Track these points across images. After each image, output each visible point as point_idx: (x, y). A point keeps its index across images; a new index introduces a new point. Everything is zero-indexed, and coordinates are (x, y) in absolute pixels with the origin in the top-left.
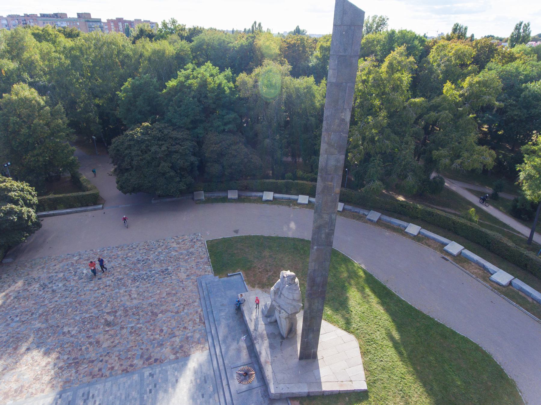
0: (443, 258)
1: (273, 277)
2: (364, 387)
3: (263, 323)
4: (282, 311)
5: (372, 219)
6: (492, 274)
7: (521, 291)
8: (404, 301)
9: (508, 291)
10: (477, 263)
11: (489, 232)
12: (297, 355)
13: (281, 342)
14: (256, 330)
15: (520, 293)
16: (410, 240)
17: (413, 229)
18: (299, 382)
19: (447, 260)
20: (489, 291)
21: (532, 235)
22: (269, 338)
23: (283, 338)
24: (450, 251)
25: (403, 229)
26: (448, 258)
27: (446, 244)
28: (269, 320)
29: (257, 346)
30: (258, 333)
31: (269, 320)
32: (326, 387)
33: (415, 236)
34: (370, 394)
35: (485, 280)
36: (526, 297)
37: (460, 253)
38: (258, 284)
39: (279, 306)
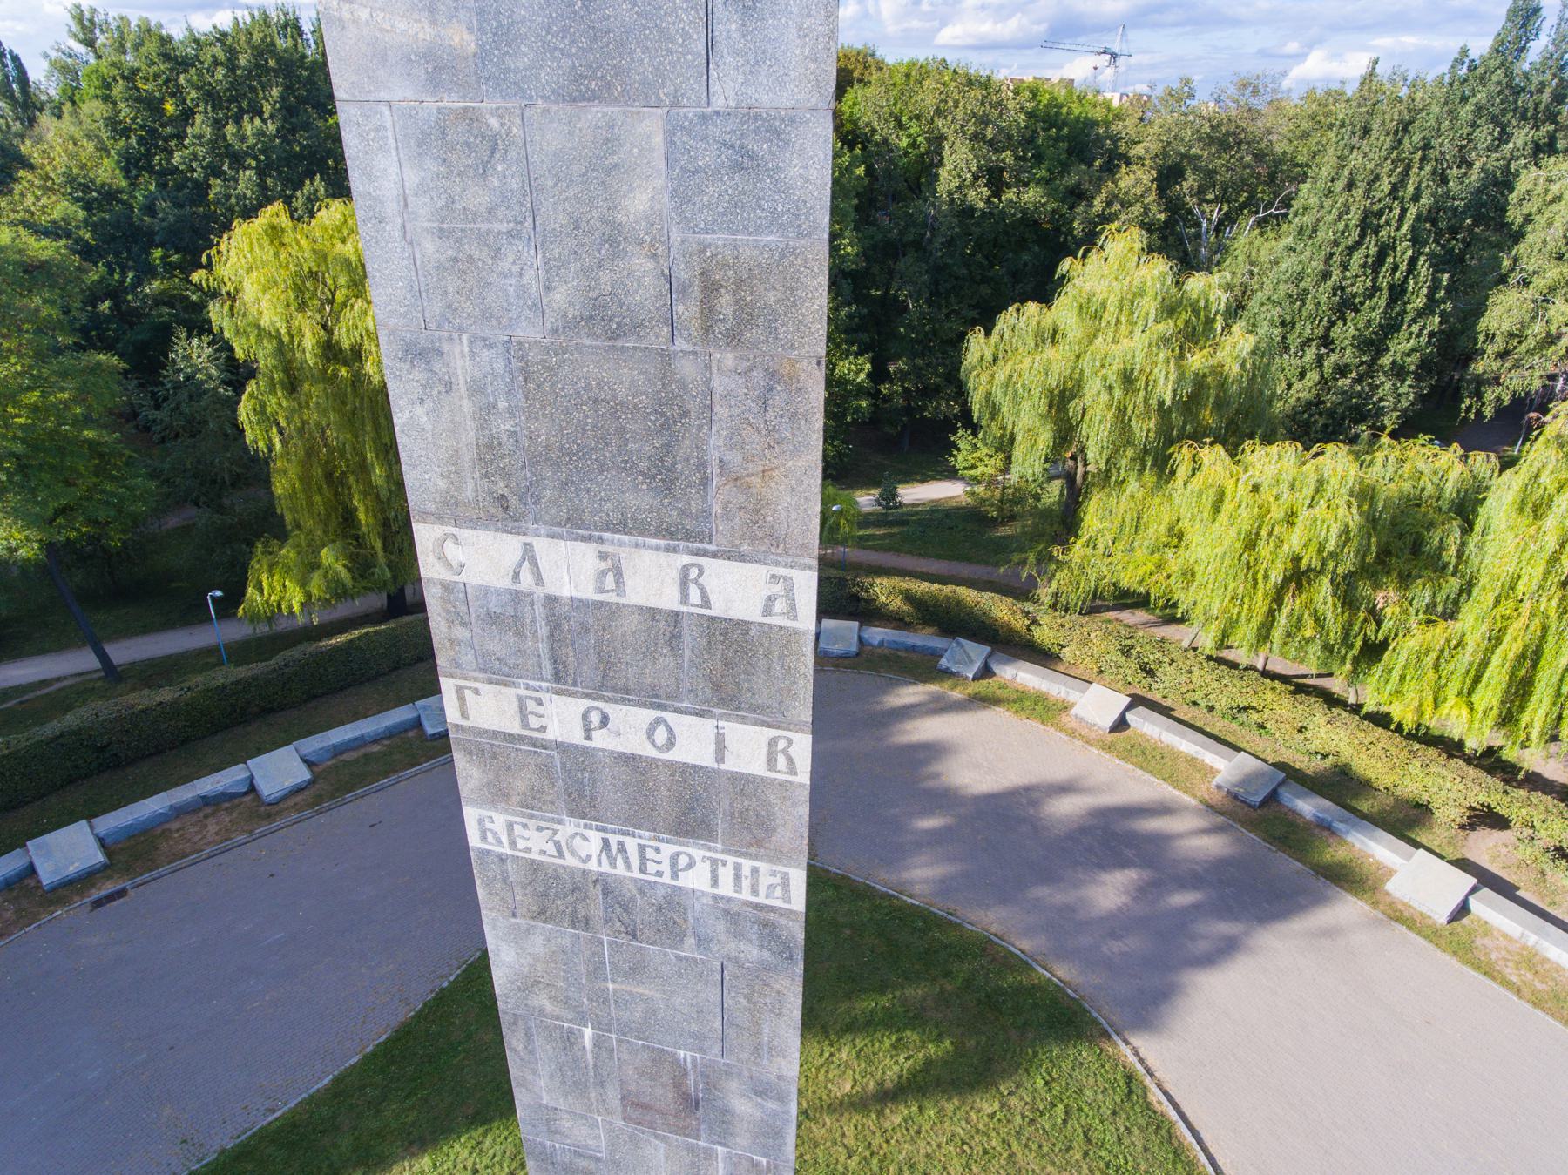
0: (98, 904)
6: (252, 789)
7: (342, 753)
8: (337, 1081)
9: (335, 781)
10: (179, 812)
11: (71, 720)
15: (346, 757)
19: (121, 893)
20: (323, 819)
21: (103, 657)
24: (72, 869)
26: (109, 887)
35: (269, 817)
36: (362, 751)
37: (102, 842)
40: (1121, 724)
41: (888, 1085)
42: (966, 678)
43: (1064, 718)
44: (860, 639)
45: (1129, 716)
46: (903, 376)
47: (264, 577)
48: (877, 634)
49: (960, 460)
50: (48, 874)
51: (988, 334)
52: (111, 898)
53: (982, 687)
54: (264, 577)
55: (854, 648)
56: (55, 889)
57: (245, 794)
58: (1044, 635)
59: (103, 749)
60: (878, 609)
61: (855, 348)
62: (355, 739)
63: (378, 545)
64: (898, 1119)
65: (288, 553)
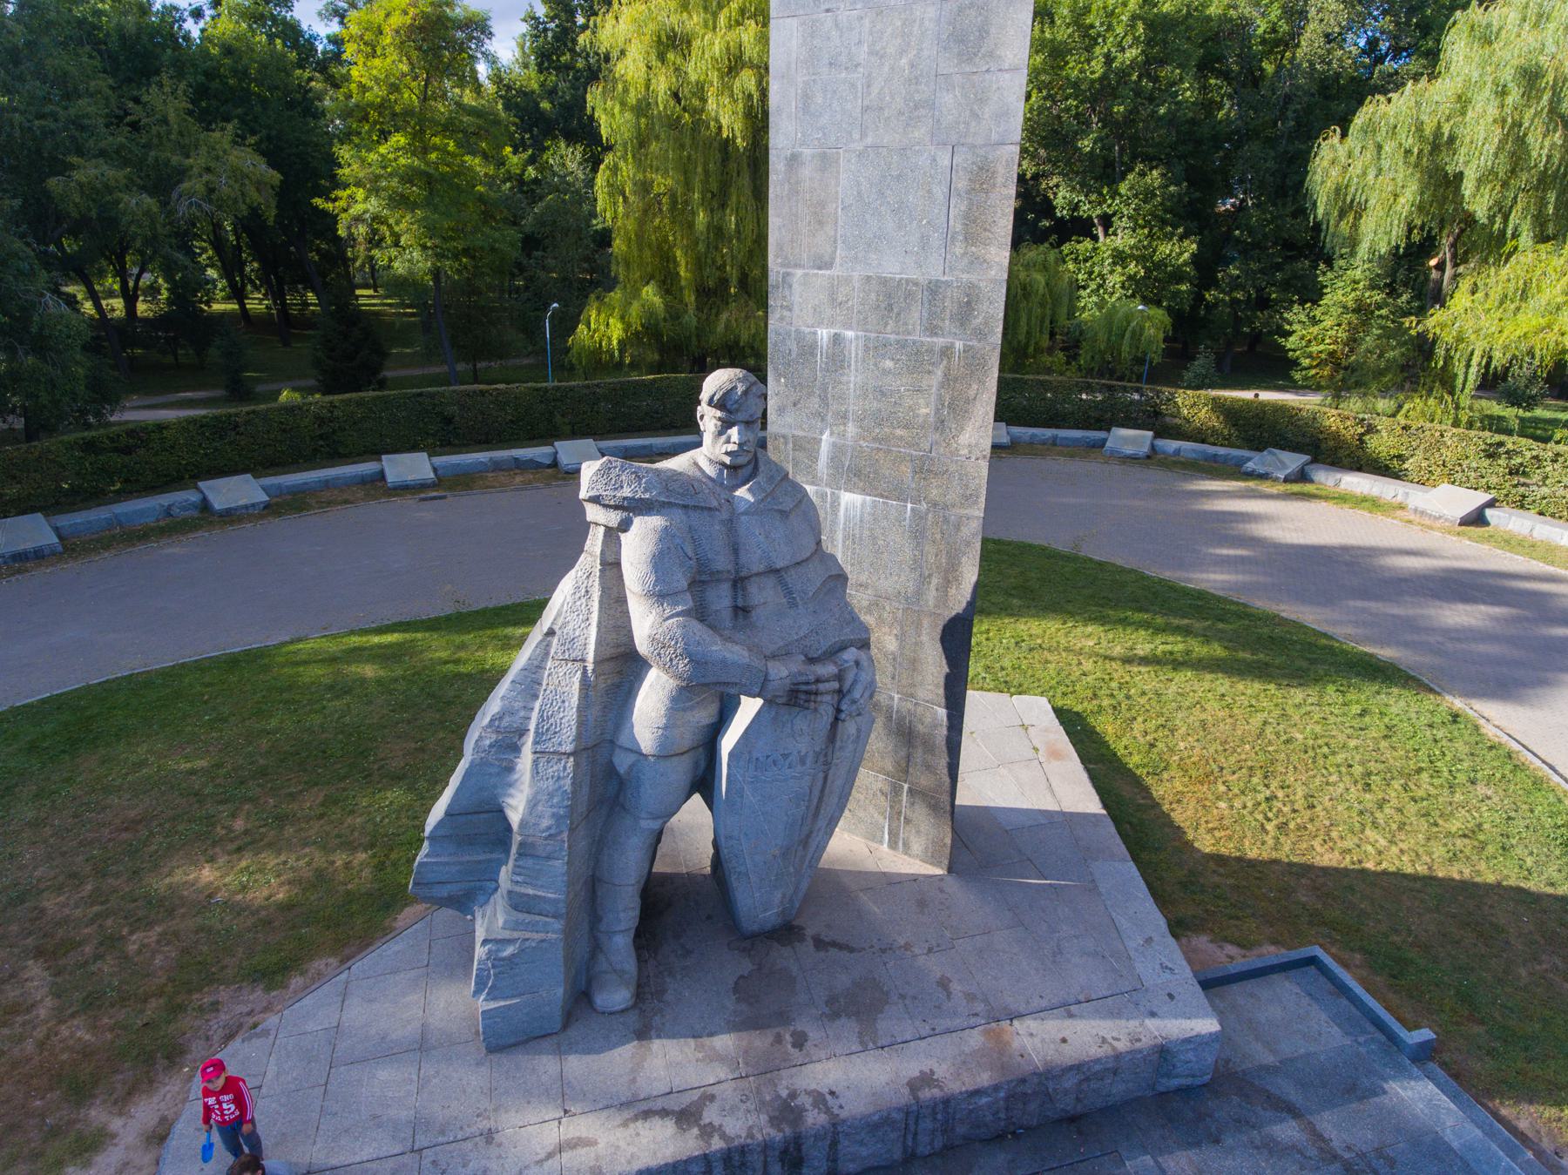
1: (107, 966)
2: (1037, 710)
3: (624, 1053)
4: (850, 654)
5: (28, 545)
6: (555, 464)
10: (497, 466)
12: (915, 879)
13: (820, 944)
14: (686, 1117)
16: (276, 524)
17: (236, 491)
18: (1093, 889)
22: (782, 1018)
23: (786, 932)
25: (196, 514)
27: (381, 475)
28: (615, 996)
29: (853, 1107)
30: (728, 1091)
31: (615, 996)
32: (1085, 800)
33: (267, 506)
34: (1060, 703)
38: (80, 1093)
39: (811, 661)
40: (1477, 519)
41: (1141, 653)
42: (1276, 480)
43: (1399, 513)
44: (1153, 447)
45: (1489, 512)
46: (1235, 284)
47: (593, 314)
48: (1171, 445)
49: (1291, 343)
50: (391, 478)
51: (1344, 135)
52: (434, 498)
53: (1296, 488)
54: (593, 314)
55: (1146, 449)
56: (395, 489)
57: (549, 466)
58: (1382, 444)
59: (448, 420)
60: (1178, 427)
61: (1181, 230)
62: (644, 447)
63: (690, 298)
64: (1143, 669)
65: (616, 295)
